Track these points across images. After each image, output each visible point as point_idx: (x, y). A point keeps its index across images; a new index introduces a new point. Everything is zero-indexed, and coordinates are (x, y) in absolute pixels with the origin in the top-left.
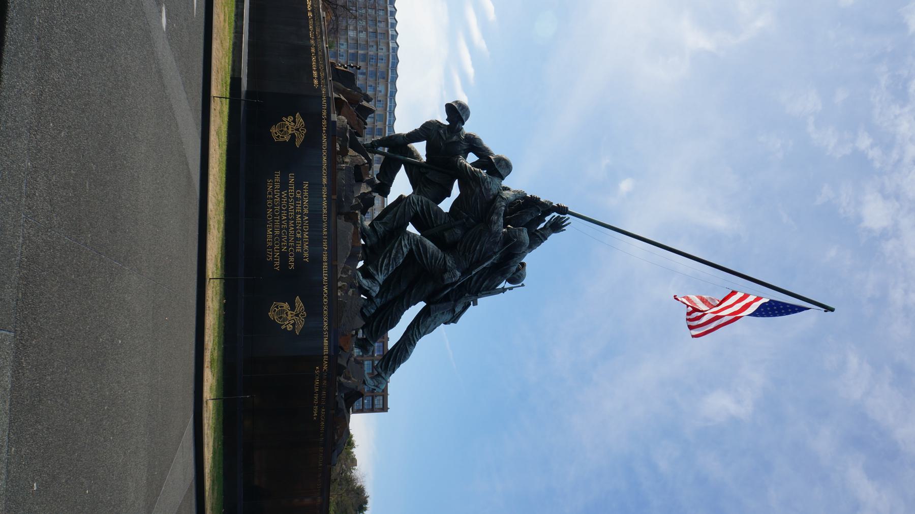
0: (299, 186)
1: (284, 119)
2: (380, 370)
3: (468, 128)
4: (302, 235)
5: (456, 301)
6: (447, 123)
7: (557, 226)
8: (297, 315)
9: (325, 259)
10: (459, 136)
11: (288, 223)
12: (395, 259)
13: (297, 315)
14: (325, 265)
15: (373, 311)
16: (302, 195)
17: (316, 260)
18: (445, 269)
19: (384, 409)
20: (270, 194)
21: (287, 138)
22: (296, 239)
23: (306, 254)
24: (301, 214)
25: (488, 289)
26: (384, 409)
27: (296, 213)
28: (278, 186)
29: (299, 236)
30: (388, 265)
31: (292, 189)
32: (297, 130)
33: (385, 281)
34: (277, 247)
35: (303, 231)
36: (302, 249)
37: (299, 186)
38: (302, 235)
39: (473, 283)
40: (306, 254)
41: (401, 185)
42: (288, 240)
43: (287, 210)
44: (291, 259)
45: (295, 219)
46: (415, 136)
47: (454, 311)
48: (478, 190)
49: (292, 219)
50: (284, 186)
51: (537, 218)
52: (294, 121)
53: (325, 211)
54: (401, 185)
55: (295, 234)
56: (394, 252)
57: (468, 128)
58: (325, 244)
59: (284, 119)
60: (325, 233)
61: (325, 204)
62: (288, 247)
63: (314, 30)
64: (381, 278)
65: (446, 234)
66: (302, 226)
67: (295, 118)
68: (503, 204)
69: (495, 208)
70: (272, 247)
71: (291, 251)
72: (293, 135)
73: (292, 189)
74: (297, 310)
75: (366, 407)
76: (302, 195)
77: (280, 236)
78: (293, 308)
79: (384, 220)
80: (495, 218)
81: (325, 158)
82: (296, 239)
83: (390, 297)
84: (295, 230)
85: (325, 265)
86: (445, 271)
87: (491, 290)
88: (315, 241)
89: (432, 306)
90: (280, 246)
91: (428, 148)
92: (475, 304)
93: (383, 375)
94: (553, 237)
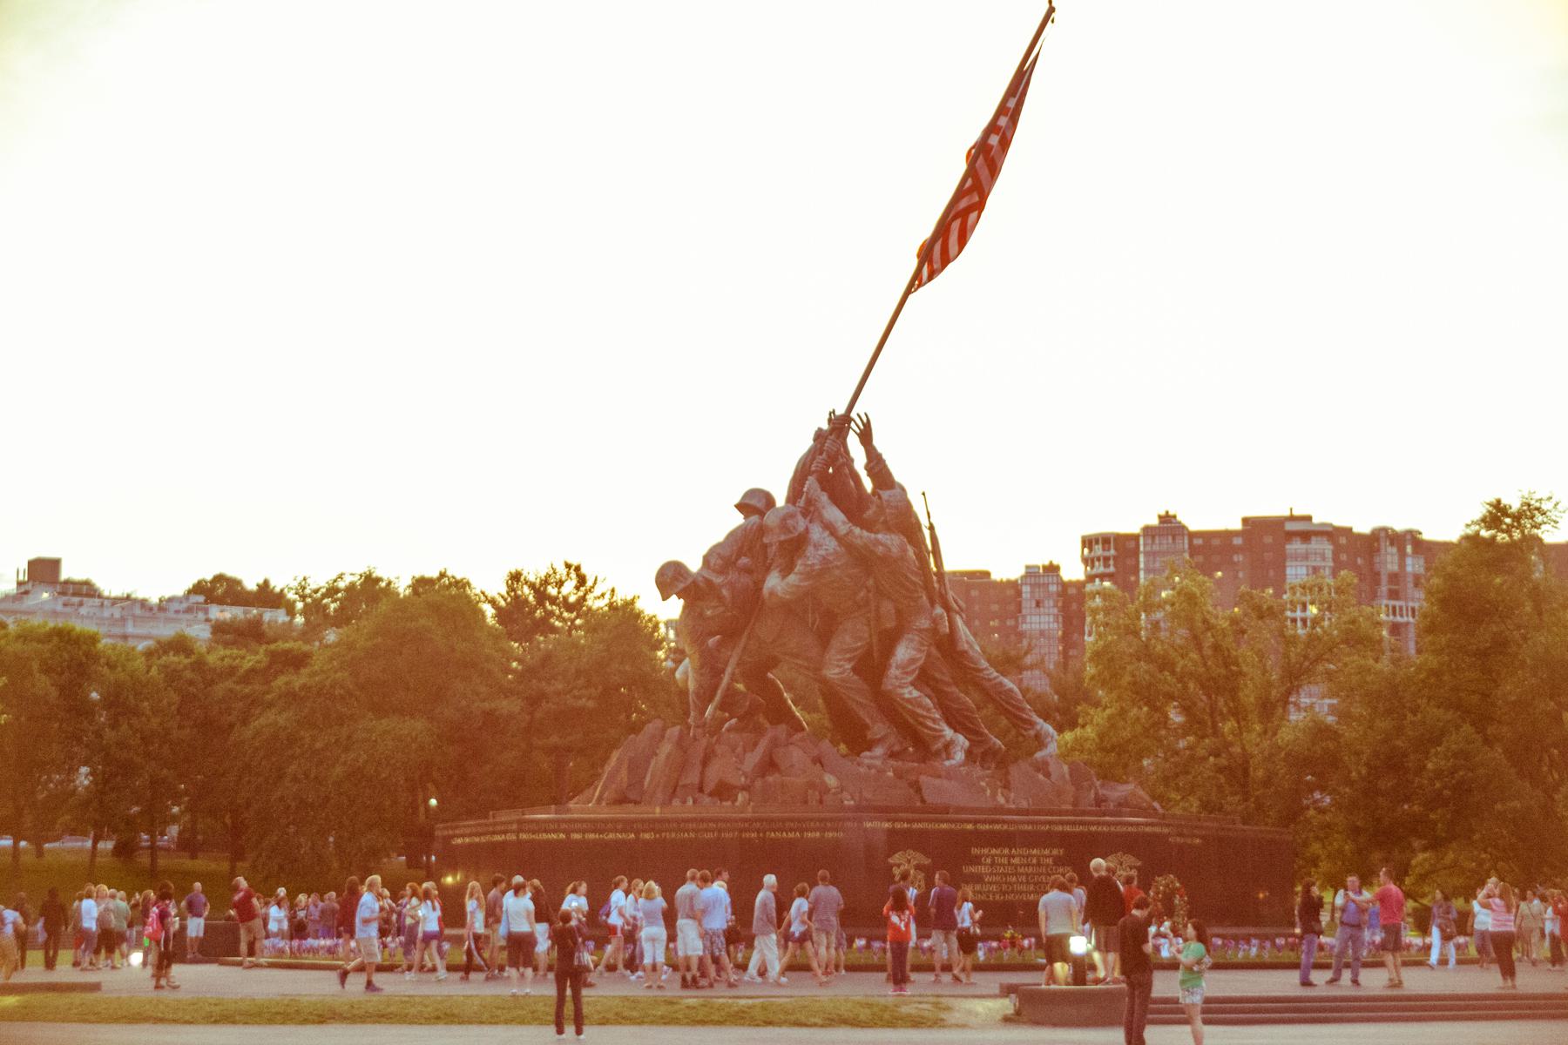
0: (976, 860)
3: (694, 565)
7: (866, 436)
12: (928, 710)
22: (1039, 864)
23: (1055, 852)
31: (983, 869)
40: (1055, 852)
43: (1005, 875)
45: (1016, 866)
48: (837, 572)
56: (919, 711)
57: (694, 565)
64: (948, 733)
68: (857, 531)
73: (983, 869)
82: (1039, 864)
91: (712, 634)
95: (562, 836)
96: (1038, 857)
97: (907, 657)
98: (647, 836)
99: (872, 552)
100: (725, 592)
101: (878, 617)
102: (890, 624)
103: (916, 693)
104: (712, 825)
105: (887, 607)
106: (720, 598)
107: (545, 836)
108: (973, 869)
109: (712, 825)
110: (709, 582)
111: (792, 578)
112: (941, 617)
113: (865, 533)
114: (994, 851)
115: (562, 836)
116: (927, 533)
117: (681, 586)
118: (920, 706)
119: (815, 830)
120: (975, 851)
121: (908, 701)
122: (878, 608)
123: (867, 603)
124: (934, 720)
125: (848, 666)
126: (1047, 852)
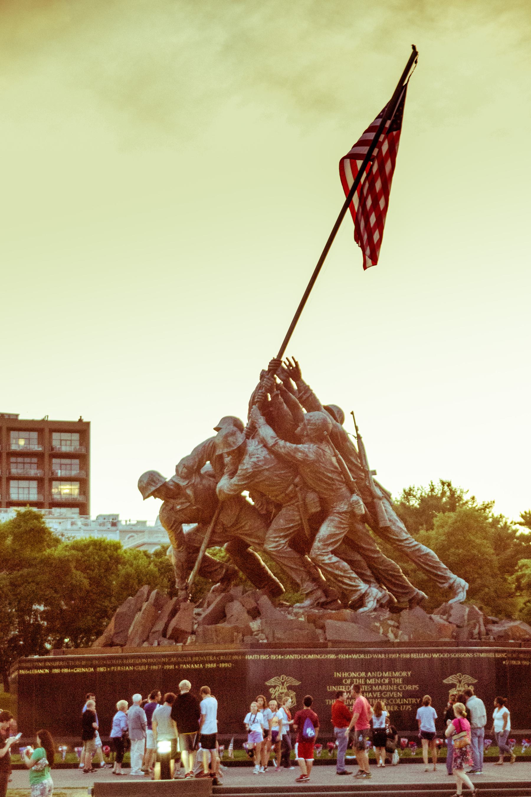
0: (339, 682)
4: (386, 678)
5: (372, 495)
7: (294, 372)
8: (460, 682)
11: (375, 691)
12: (345, 571)
13: (460, 682)
16: (348, 678)
17: (408, 664)
18: (352, 514)
19: (82, 429)
22: (390, 684)
23: (404, 674)
24: (366, 678)
26: (82, 429)
27: (366, 684)
29: (387, 681)
30: (350, 578)
31: (342, 689)
32: (283, 684)
34: (398, 701)
35: (382, 677)
36: (399, 677)
37: (339, 682)
38: (386, 678)
40: (404, 674)
42: (391, 691)
44: (409, 688)
45: (371, 685)
48: (266, 473)
49: (371, 687)
52: (275, 687)
53: (362, 656)
55: (386, 684)
56: (337, 572)
61: (355, 656)
62: (398, 691)
63: (134, 665)
64: (363, 587)
65: (313, 510)
66: (378, 678)
67: (271, 687)
68: (282, 443)
69: (288, 454)
70: (399, 705)
71: (401, 688)
72: (289, 688)
73: (342, 689)
74: (455, 682)
75: (74, 473)
76: (348, 678)
77: (388, 699)
78: (453, 686)
80: (299, 456)
82: (390, 684)
83: (369, 573)
84: (381, 684)
85: (414, 656)
87: (361, 455)
88: (392, 665)
89: (381, 525)
90: (398, 698)
92: (374, 473)
95: (47, 671)
96: (390, 678)
97: (328, 533)
98: (102, 669)
99: (294, 458)
100: (189, 492)
101: (305, 504)
103: (335, 559)
104: (144, 660)
105: (311, 497)
106: (187, 497)
107: (36, 672)
108: (334, 688)
109: (144, 660)
110: (177, 486)
111: (235, 480)
112: (357, 502)
113: (288, 444)
114: (353, 674)
115: (47, 671)
116: (355, 442)
117: (153, 489)
118: (338, 568)
119: (213, 662)
121: (328, 565)
122: (304, 500)
123: (296, 496)
124: (350, 578)
126: (397, 674)
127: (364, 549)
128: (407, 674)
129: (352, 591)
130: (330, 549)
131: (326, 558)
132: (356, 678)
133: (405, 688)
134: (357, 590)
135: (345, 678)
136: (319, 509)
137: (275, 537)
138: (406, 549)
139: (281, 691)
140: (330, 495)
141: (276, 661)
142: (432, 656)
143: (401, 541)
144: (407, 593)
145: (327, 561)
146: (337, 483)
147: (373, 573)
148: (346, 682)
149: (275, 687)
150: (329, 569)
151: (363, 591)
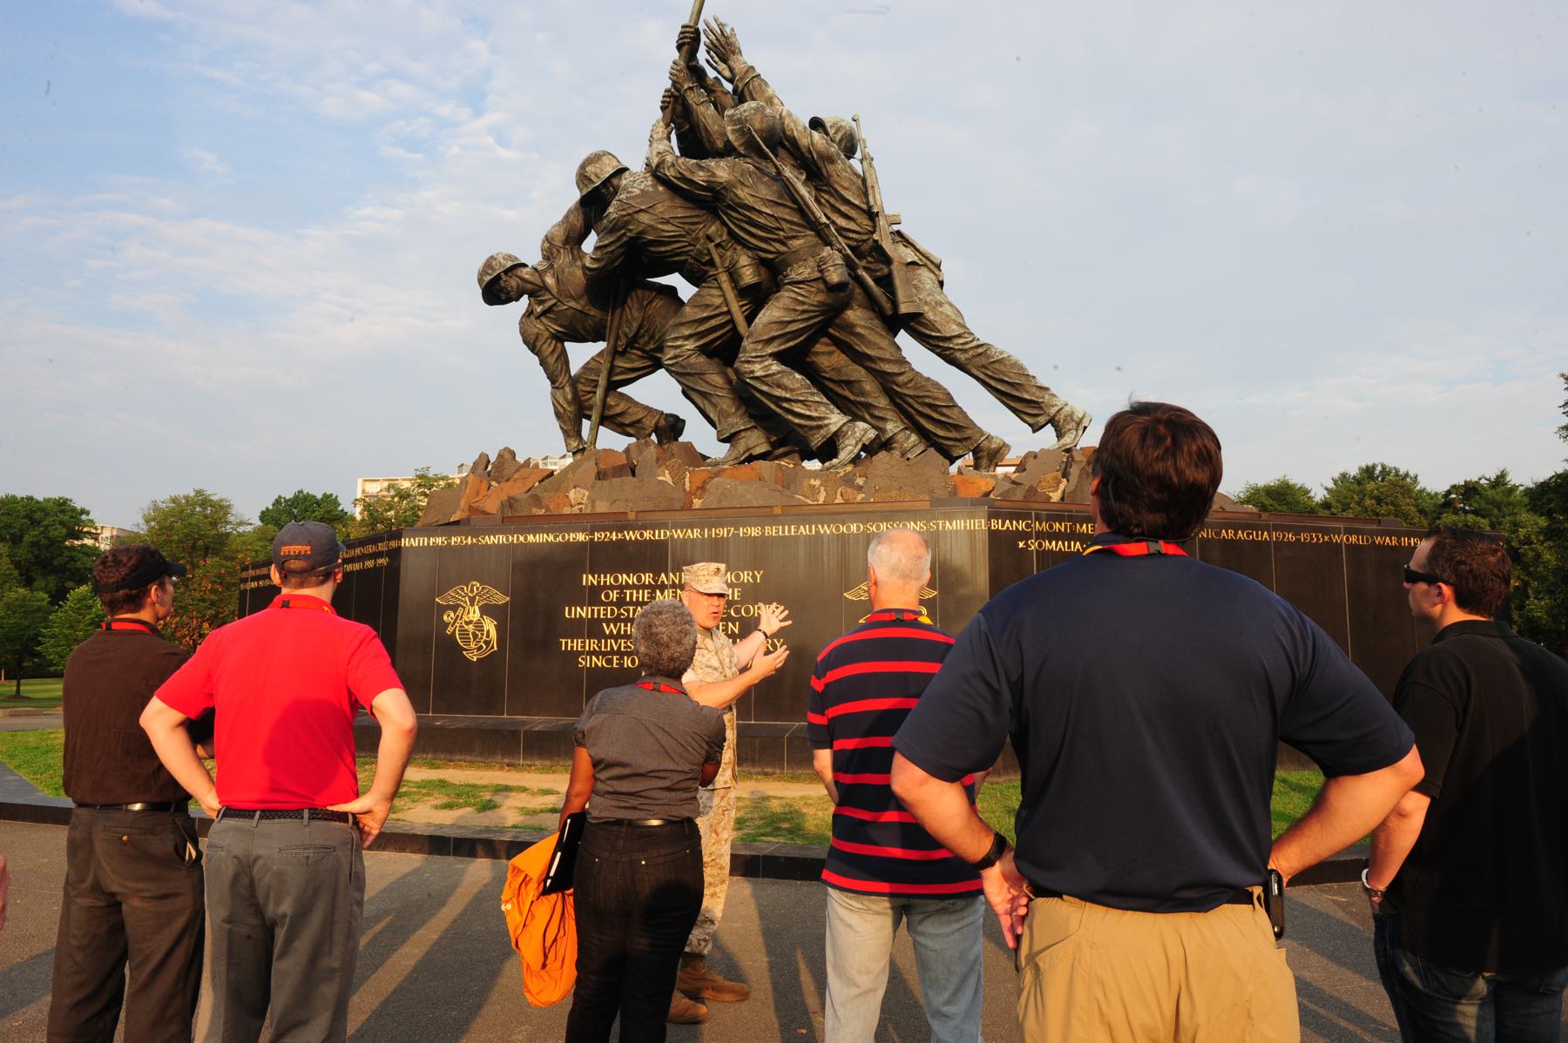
0: (593, 596)
1: (449, 630)
2: (1042, 420)
5: (888, 261)
6: (525, 300)
7: (724, 49)
9: (754, 532)
10: (545, 271)
12: (792, 390)
14: (771, 531)
15: (914, 438)
16: (612, 588)
20: (609, 662)
21: (490, 626)
24: (652, 588)
25: (865, 194)
28: (592, 644)
31: (601, 612)
33: (843, 411)
39: (852, 226)
40: (746, 577)
41: (657, 392)
46: (555, 368)
47: (913, 263)
50: (593, 629)
51: (702, 86)
54: (657, 392)
56: (778, 392)
58: (723, 532)
59: (449, 630)
60: (696, 533)
64: (836, 420)
67: (448, 607)
71: (737, 611)
73: (601, 612)
76: (612, 588)
79: (715, 419)
81: (531, 538)
83: (882, 402)
86: (822, 279)
87: (864, 188)
91: (580, 339)
93: (1053, 411)
94: (752, 55)
102: (748, 276)
103: (776, 367)
108: (583, 612)
114: (623, 578)
120: (588, 579)
123: (711, 263)
125: (691, 345)
127: (869, 358)
128: (754, 577)
129: (812, 428)
130: (771, 349)
131: (758, 366)
132: (634, 587)
133: (747, 611)
134: (820, 427)
135: (605, 587)
136: (755, 280)
137: (676, 339)
138: (958, 355)
139: (465, 618)
140: (779, 253)
141: (462, 548)
142: (817, 532)
143: (949, 339)
144: (966, 439)
145: (758, 374)
146: (785, 226)
147: (892, 401)
148: (607, 596)
149: (455, 608)
150: (765, 388)
151: (834, 429)
